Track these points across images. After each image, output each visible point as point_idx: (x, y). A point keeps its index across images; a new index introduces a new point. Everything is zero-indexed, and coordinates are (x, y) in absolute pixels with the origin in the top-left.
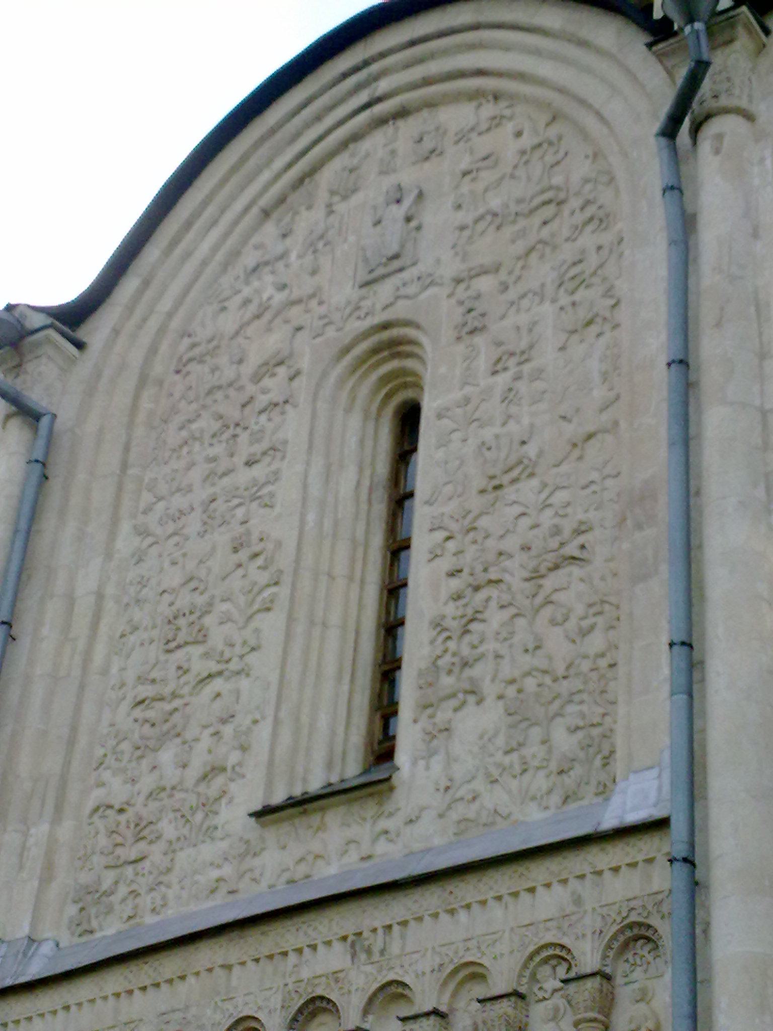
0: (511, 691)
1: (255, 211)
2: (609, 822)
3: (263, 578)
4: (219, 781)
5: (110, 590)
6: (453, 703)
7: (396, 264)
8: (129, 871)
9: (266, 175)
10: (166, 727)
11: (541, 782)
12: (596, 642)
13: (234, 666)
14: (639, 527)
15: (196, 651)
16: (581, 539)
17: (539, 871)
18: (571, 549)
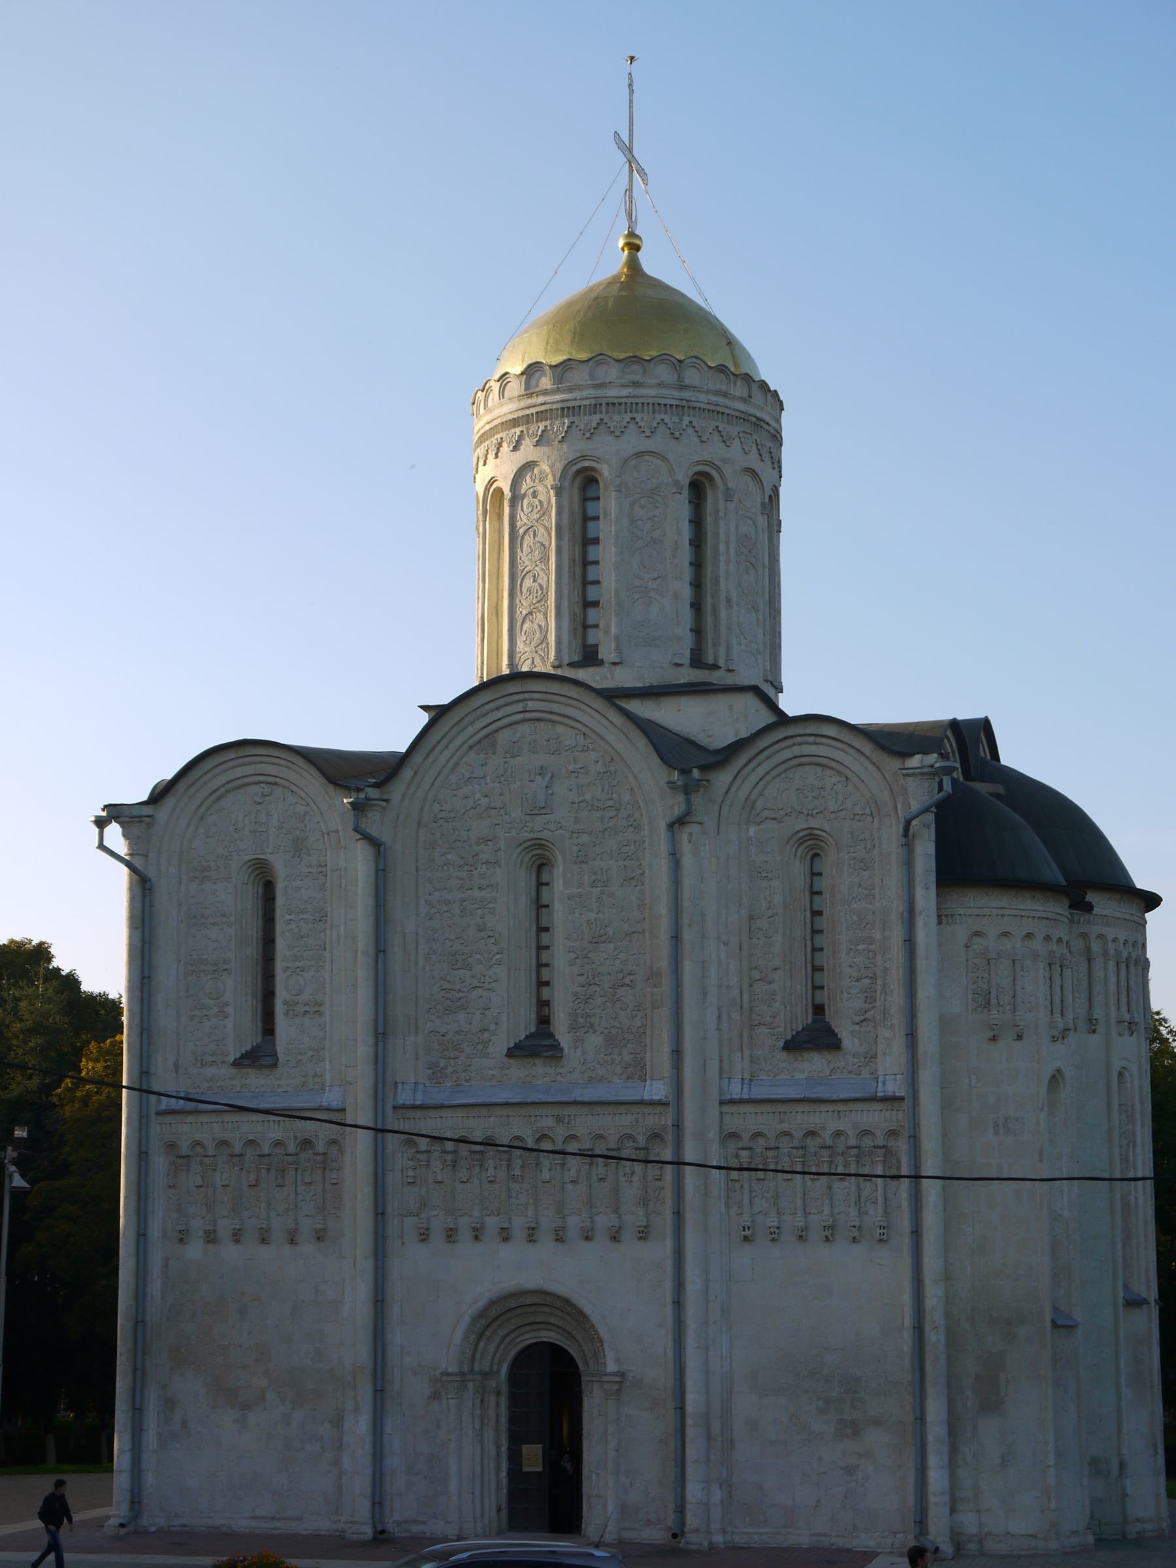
0: (606, 1031)
1: (466, 746)
2: (647, 1097)
3: (495, 949)
4: (486, 1035)
5: (420, 932)
6: (584, 1030)
7: (543, 811)
8: (452, 1062)
9: (471, 730)
10: (459, 1004)
11: (619, 1070)
12: (638, 1022)
13: (486, 985)
14: (656, 986)
15: (468, 973)
16: (631, 977)
17: (623, 1109)
18: (627, 981)
